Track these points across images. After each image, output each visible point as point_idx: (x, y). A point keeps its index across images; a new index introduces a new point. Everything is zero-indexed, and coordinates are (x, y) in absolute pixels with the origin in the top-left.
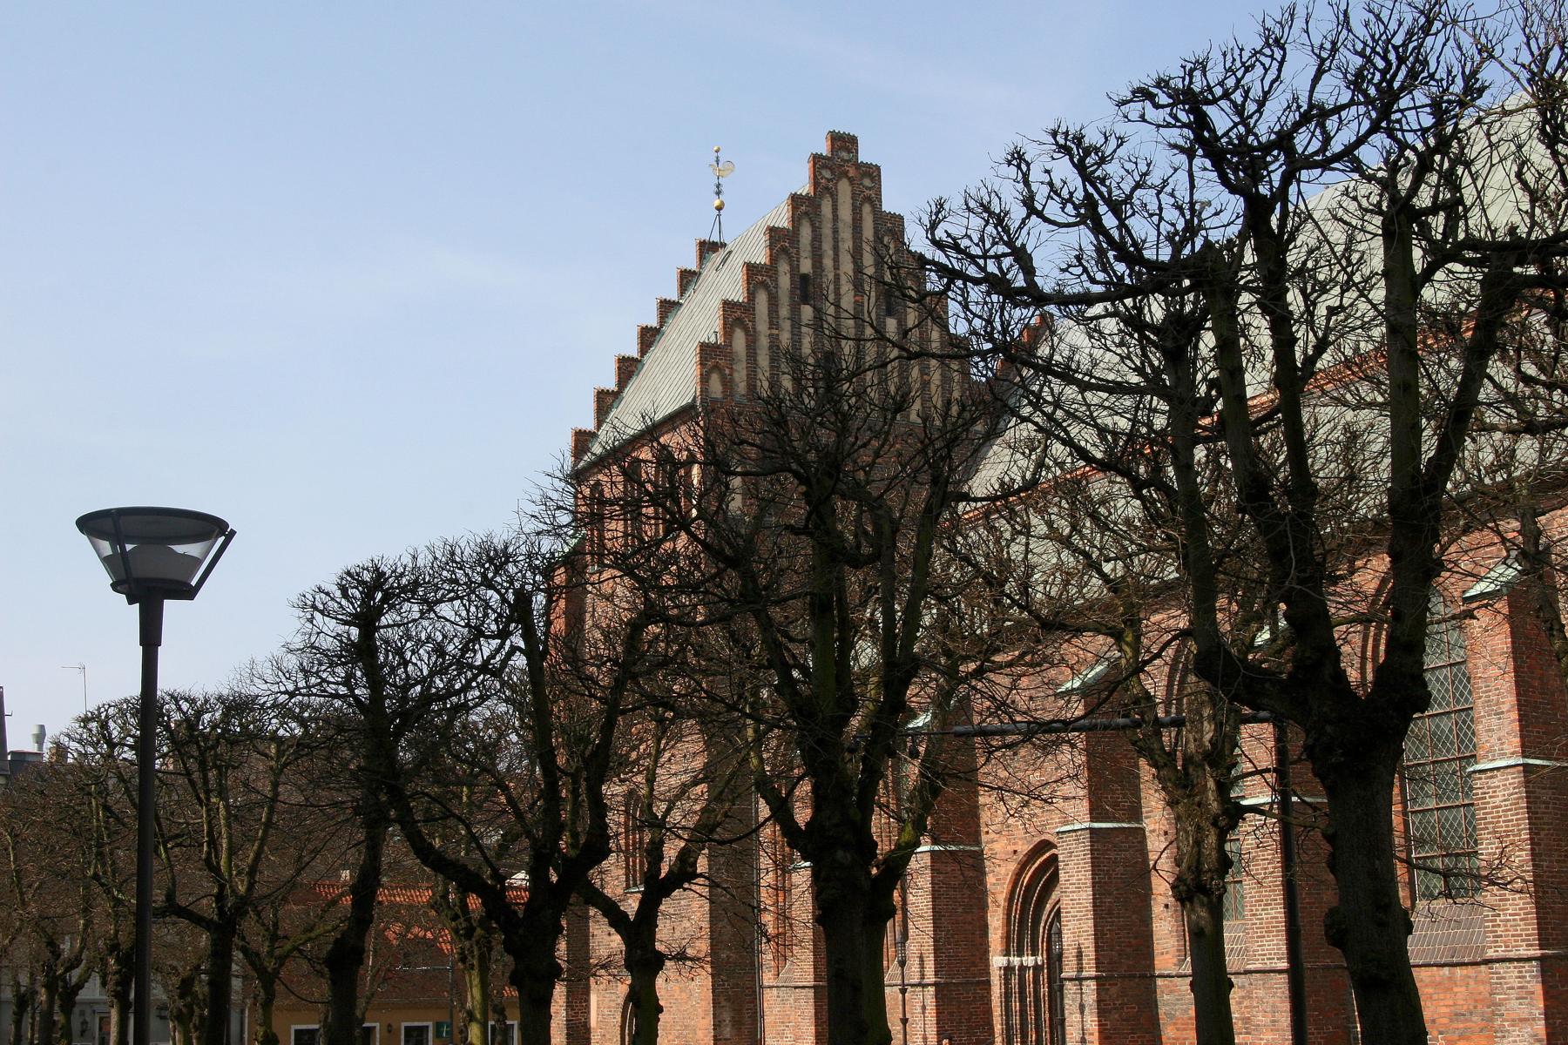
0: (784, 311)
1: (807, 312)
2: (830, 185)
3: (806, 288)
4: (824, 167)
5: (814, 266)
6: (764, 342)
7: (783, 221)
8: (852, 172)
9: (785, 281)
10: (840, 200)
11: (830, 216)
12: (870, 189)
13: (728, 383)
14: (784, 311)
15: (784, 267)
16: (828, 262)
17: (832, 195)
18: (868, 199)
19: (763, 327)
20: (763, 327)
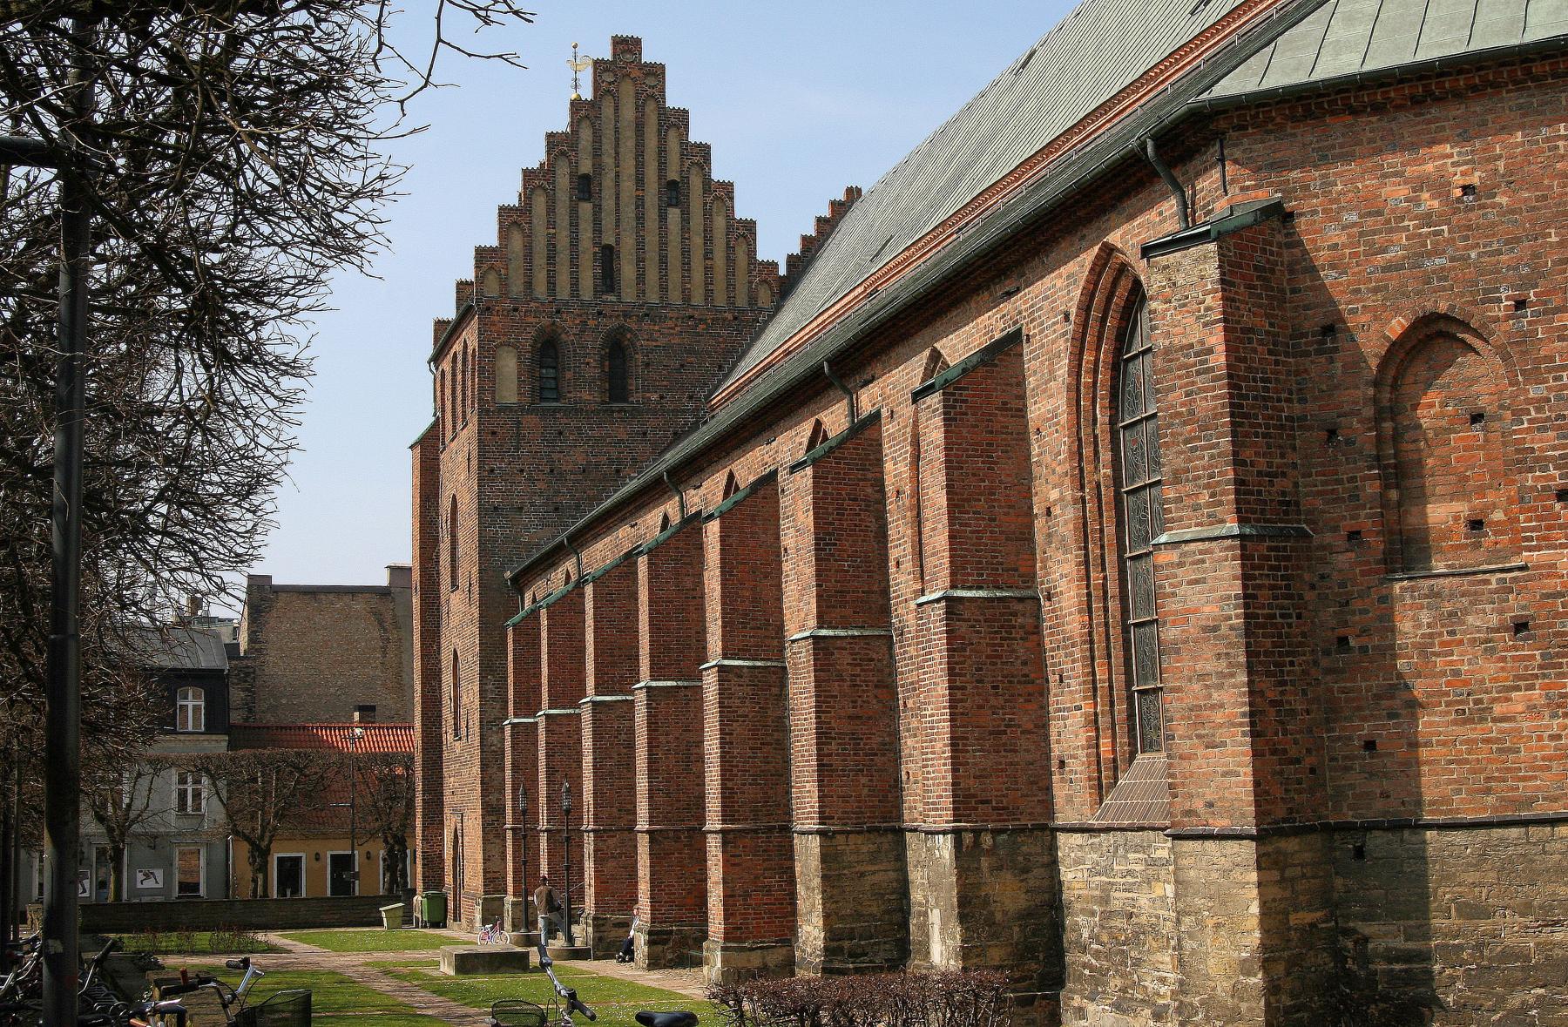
3: (585, 187)
4: (606, 70)
9: (563, 181)
13: (504, 283)
16: (608, 161)
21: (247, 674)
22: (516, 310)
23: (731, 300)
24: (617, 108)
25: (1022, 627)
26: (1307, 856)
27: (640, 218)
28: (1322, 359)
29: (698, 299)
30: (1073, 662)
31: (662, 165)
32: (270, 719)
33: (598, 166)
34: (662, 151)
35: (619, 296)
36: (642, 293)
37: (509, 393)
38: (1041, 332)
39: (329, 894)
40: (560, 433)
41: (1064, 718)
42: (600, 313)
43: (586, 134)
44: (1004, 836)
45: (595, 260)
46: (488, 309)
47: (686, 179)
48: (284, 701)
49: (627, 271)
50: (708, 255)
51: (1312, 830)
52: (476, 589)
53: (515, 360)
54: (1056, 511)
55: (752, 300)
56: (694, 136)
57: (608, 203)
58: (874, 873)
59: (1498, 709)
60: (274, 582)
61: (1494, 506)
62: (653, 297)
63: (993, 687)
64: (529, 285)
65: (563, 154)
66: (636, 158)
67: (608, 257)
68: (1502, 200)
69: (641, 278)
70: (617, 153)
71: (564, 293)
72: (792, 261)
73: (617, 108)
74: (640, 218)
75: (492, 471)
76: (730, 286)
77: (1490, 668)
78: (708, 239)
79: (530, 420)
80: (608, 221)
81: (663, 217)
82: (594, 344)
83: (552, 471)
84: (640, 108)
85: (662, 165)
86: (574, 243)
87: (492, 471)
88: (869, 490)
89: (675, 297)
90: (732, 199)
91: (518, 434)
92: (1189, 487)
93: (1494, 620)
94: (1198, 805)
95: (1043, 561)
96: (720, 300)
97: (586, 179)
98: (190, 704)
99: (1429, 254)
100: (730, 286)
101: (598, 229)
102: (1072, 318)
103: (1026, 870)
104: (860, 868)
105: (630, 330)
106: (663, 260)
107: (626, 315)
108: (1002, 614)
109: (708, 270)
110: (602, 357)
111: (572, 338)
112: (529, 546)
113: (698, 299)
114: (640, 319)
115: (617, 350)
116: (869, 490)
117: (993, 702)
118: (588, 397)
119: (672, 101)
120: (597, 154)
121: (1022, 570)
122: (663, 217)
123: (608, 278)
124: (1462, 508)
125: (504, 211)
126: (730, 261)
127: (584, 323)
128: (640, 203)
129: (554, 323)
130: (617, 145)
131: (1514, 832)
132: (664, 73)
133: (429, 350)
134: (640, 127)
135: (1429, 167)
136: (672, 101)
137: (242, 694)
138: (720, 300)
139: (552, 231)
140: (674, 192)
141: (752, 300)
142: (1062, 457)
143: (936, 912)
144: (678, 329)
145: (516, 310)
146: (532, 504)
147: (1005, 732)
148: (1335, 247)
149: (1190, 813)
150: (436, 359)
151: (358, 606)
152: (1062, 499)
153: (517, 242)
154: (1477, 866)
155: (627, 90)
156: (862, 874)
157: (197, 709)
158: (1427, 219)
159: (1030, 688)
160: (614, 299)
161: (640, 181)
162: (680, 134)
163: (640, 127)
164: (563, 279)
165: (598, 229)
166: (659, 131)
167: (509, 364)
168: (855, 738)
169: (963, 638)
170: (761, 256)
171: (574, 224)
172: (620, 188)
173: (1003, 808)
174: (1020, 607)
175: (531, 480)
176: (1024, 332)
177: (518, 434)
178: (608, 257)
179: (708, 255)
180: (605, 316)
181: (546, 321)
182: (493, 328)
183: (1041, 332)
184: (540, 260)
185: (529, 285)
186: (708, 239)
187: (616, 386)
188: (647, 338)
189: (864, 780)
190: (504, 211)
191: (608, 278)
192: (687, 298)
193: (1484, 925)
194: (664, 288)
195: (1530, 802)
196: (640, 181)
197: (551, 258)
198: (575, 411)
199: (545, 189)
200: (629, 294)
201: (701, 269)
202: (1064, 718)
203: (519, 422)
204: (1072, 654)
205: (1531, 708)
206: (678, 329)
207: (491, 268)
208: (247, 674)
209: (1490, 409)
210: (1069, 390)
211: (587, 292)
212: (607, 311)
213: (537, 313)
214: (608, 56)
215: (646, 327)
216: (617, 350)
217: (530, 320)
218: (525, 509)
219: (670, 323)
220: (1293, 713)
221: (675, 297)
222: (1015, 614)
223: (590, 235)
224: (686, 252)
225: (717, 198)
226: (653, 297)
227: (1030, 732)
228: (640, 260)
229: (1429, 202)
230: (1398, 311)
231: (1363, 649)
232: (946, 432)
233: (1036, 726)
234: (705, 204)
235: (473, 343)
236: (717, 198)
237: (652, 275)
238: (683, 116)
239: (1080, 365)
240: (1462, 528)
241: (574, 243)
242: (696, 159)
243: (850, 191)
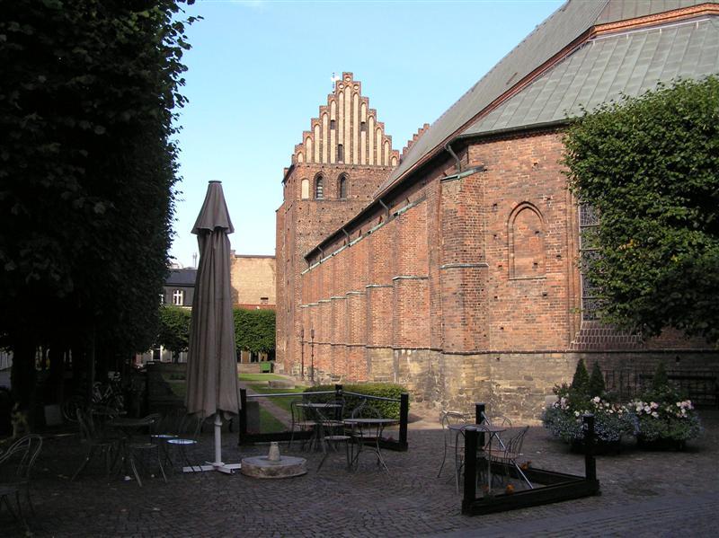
0: (325, 132)
3: (333, 124)
6: (317, 143)
8: (351, 85)
9: (325, 123)
13: (305, 157)
14: (325, 132)
15: (325, 118)
16: (341, 115)
23: (383, 163)
26: (482, 361)
27: (352, 135)
28: (493, 214)
29: (371, 163)
31: (360, 116)
33: (338, 117)
34: (360, 112)
37: (306, 194)
47: (368, 121)
49: (347, 153)
50: (375, 147)
51: (484, 353)
55: (390, 163)
59: (538, 320)
61: (540, 260)
62: (356, 162)
64: (313, 158)
67: (340, 147)
68: (545, 168)
69: (352, 156)
71: (325, 161)
72: (405, 150)
74: (352, 135)
76: (383, 158)
77: (535, 307)
78: (375, 142)
79: (312, 204)
80: (341, 137)
81: (360, 135)
82: (335, 178)
84: (352, 97)
85: (360, 116)
86: (329, 144)
89: (363, 162)
92: (451, 252)
93: (537, 294)
94: (450, 345)
96: (379, 163)
97: (333, 121)
99: (524, 184)
100: (383, 158)
106: (359, 150)
109: (375, 153)
112: (311, 247)
113: (371, 163)
114: (351, 170)
115: (342, 178)
120: (337, 113)
122: (360, 135)
123: (340, 156)
124: (532, 259)
126: (383, 150)
128: (352, 129)
131: (541, 355)
133: (282, 178)
134: (352, 104)
135: (525, 157)
138: (379, 163)
140: (363, 126)
141: (390, 163)
148: (498, 180)
149: (448, 347)
150: (284, 181)
151: (266, 261)
153: (309, 142)
154: (530, 365)
158: (524, 173)
161: (352, 122)
163: (352, 104)
167: (306, 185)
168: (384, 319)
170: (393, 148)
171: (329, 137)
172: (345, 124)
174: (421, 281)
178: (340, 147)
179: (375, 147)
184: (317, 148)
185: (313, 158)
186: (375, 142)
187: (341, 192)
188: (353, 176)
191: (340, 156)
192: (367, 163)
193: (531, 383)
194: (360, 159)
195: (545, 347)
196: (352, 122)
198: (327, 201)
200: (347, 161)
205: (547, 319)
209: (540, 230)
211: (333, 161)
213: (316, 168)
216: (342, 178)
220: (479, 319)
221: (363, 162)
224: (367, 147)
226: (356, 162)
228: (352, 150)
229: (525, 168)
230: (515, 200)
231: (501, 300)
240: (532, 265)
241: (329, 144)
243: (425, 125)
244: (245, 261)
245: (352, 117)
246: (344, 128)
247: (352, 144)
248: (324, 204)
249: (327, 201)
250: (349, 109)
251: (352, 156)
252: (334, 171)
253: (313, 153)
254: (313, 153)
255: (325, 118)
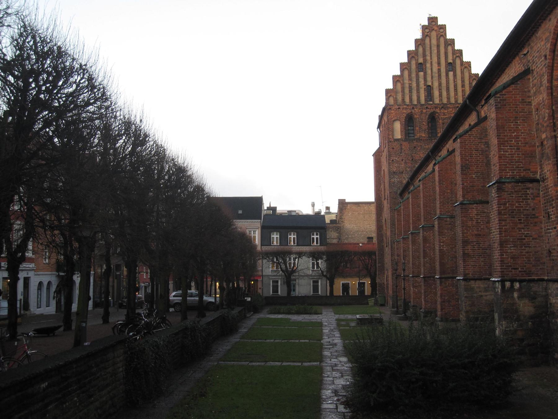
0: (414, 75)
1: (421, 74)
2: (428, 34)
4: (427, 28)
5: (423, 59)
6: (407, 85)
7: (413, 48)
8: (436, 28)
9: (414, 66)
10: (432, 38)
11: (429, 43)
12: (442, 32)
13: (396, 100)
14: (414, 75)
16: (428, 58)
17: (429, 37)
18: (442, 36)
19: (407, 81)
20: (407, 81)
21: (338, 228)
22: (399, 108)
24: (430, 40)
25: (532, 194)
27: (440, 76)
30: (553, 208)
32: (346, 241)
33: (425, 60)
35: (433, 102)
36: (441, 100)
37: (398, 135)
38: (537, 67)
39: (358, 295)
40: (415, 147)
41: (550, 233)
42: (427, 108)
43: (421, 50)
44: (525, 283)
45: (425, 91)
46: (390, 109)
48: (350, 236)
49: (436, 93)
50: (463, 86)
52: (389, 199)
53: (400, 124)
54: (545, 143)
56: (457, 48)
57: (429, 72)
58: (486, 296)
60: (347, 201)
63: (519, 220)
64: (403, 100)
65: (413, 57)
66: (438, 56)
67: (429, 89)
69: (441, 95)
70: (431, 55)
73: (430, 40)
74: (440, 76)
75: (393, 160)
78: (463, 81)
79: (404, 143)
80: (429, 79)
81: (447, 75)
82: (425, 118)
83: (412, 160)
84: (438, 40)
87: (393, 160)
88: (483, 146)
90: (470, 67)
91: (401, 149)
95: (541, 165)
97: (421, 64)
98: (315, 237)
101: (425, 80)
102: (548, 57)
103: (534, 298)
104: (480, 294)
105: (437, 113)
107: (436, 108)
108: (523, 189)
110: (428, 123)
111: (418, 116)
114: (440, 109)
116: (483, 146)
117: (519, 226)
118: (424, 135)
119: (449, 37)
120: (424, 55)
121: (532, 170)
122: (447, 75)
125: (394, 77)
127: (422, 111)
128: (439, 70)
129: (412, 112)
130: (431, 53)
132: (446, 28)
134: (438, 46)
136: (449, 37)
137: (337, 234)
139: (410, 82)
140: (451, 66)
142: (546, 119)
143: (497, 314)
144: (453, 111)
145: (399, 108)
146: (406, 171)
147: (524, 239)
152: (547, 137)
153: (399, 85)
155: (434, 34)
156: (482, 296)
157: (317, 238)
159: (536, 220)
160: (431, 103)
161: (439, 64)
162: (452, 47)
163: (438, 46)
164: (415, 98)
165: (425, 80)
166: (445, 48)
167: (397, 126)
169: (505, 199)
171: (418, 80)
172: (432, 67)
173: (524, 271)
175: (405, 163)
176: (531, 69)
177: (401, 149)
178: (429, 89)
179: (463, 86)
180: (428, 108)
181: (410, 111)
182: (392, 115)
183: (537, 67)
184: (407, 91)
185: (403, 100)
186: (463, 81)
189: (482, 259)
190: (394, 77)
192: (456, 101)
194: (448, 98)
196: (439, 64)
197: (411, 91)
199: (407, 69)
200: (437, 101)
201: (461, 91)
202: (550, 233)
203: (401, 144)
204: (552, 204)
206: (453, 111)
207: (391, 96)
208: (338, 228)
210: (548, 89)
211: (423, 101)
212: (429, 107)
213: (406, 109)
214: (427, 24)
215: (442, 111)
217: (403, 111)
218: (404, 172)
219: (451, 110)
221: (453, 100)
222: (528, 188)
223: (423, 82)
224: (455, 86)
225: (466, 67)
226: (445, 101)
227: (536, 239)
232: (496, 113)
233: (539, 236)
234: (461, 69)
235: (386, 120)
236: (466, 67)
237: (444, 94)
238: (452, 41)
239: (552, 77)
242: (457, 55)
244: (354, 207)
245: (439, 58)
246: (432, 69)
247: (440, 85)
248: (415, 143)
249: (419, 140)
250: (436, 51)
251: (441, 95)
252: (424, 111)
253: (403, 95)
254: (403, 95)
255: (413, 62)
